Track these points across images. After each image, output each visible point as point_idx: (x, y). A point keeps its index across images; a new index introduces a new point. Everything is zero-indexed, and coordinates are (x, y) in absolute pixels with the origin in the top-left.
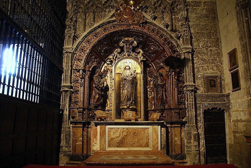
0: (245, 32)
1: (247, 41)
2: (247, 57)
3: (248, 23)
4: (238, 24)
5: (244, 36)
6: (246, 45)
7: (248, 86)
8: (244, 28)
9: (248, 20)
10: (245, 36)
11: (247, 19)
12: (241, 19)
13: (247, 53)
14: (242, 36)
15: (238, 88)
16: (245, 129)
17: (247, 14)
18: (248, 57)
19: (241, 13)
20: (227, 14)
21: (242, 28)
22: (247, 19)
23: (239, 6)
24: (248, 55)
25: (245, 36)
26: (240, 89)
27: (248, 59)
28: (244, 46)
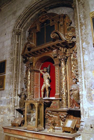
0: (15, 50)
1: (15, 57)
2: (13, 68)
3: (18, 45)
4: (12, 44)
5: (13, 53)
6: (14, 60)
7: (10, 89)
8: (15, 47)
9: (18, 43)
10: (14, 53)
11: (18, 42)
12: (15, 41)
13: (14, 65)
14: (12, 53)
15: (2, 89)
16: (3, 121)
17: (19, 39)
18: (13, 68)
19: (15, 37)
20: (5, 34)
21: (14, 47)
22: (18, 42)
23: (14, 32)
24: (14, 67)
25: (14, 53)
26: (4, 90)
27: (13, 69)
28: (12, 60)
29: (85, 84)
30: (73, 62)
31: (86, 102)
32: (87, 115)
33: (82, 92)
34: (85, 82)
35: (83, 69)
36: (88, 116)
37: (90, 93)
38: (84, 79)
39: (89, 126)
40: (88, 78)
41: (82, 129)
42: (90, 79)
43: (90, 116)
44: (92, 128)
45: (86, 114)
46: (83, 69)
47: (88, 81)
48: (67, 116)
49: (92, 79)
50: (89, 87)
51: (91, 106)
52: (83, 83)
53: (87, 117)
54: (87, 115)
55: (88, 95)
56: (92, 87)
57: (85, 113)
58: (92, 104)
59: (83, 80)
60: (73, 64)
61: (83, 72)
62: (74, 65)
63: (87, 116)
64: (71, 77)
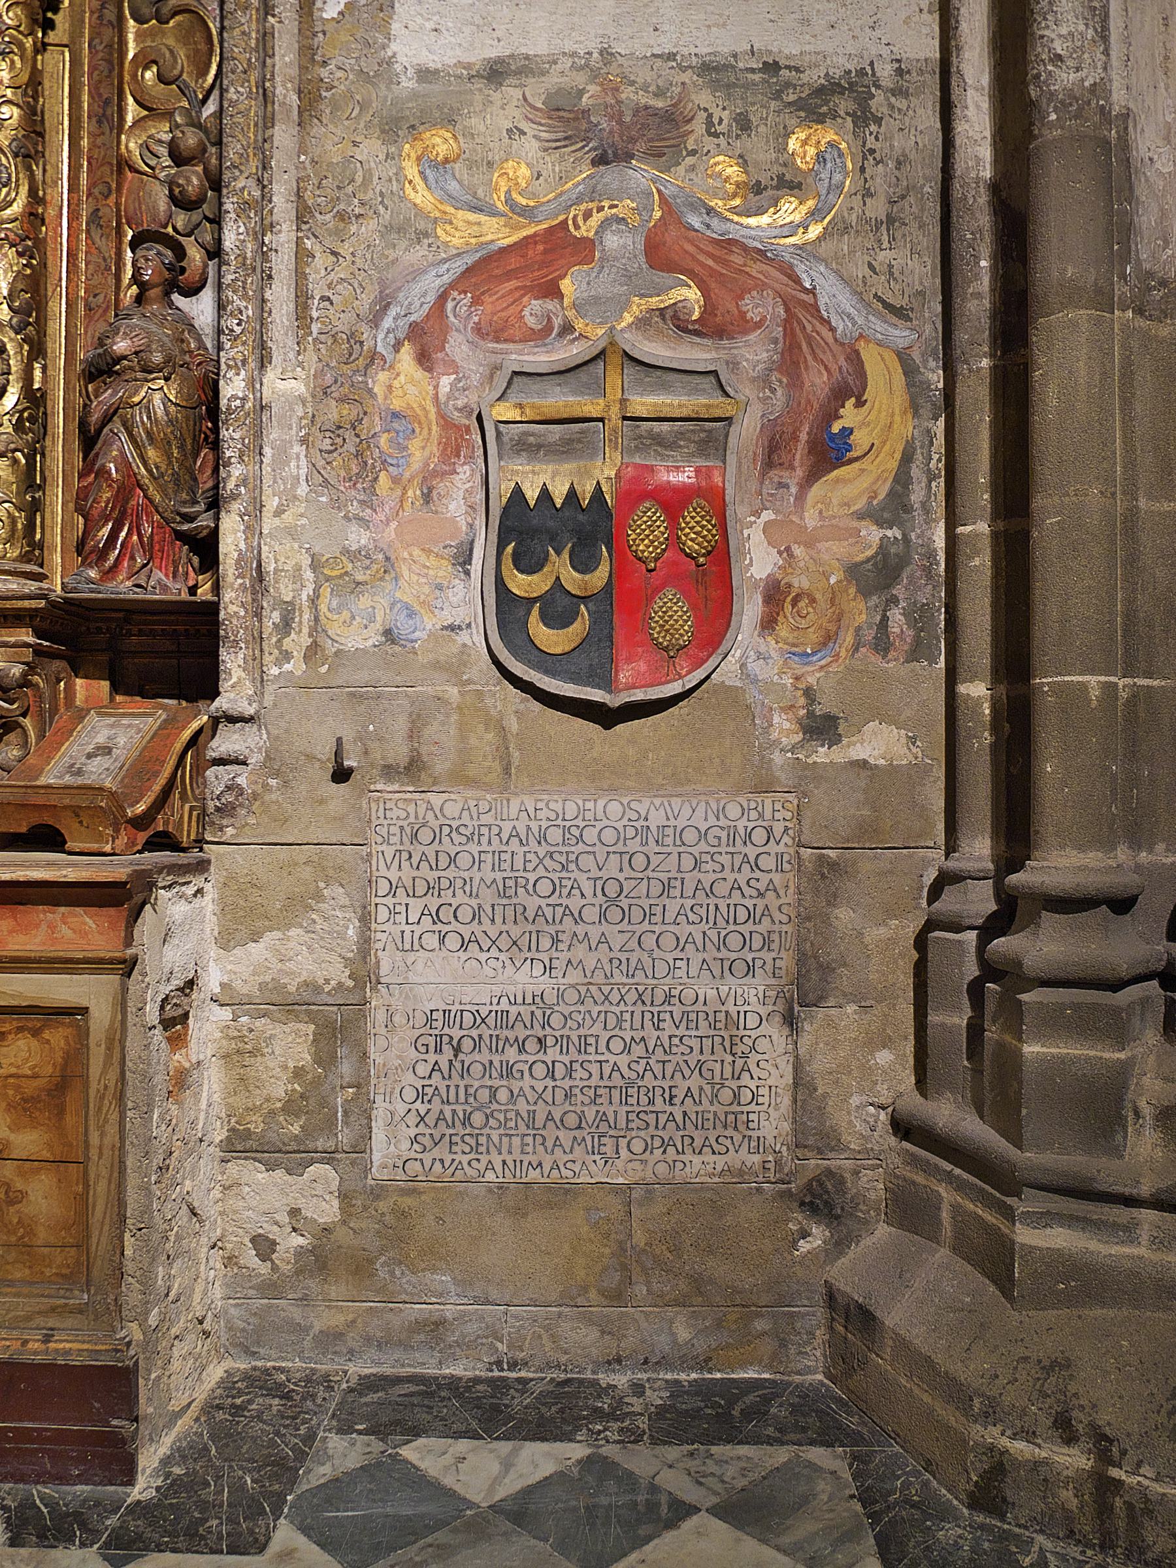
29: (300, 277)
30: (139, 36)
31: (302, 490)
32: (298, 641)
33: (251, 383)
34: (302, 255)
35: (285, 93)
36: (313, 652)
37: (357, 396)
38: (300, 220)
39: (310, 757)
40: (342, 217)
41: (229, 798)
42: (368, 229)
43: (331, 648)
44: (341, 775)
45: (285, 626)
46: (285, 93)
47: (345, 249)
48: (31, 668)
49: (389, 228)
50: (343, 322)
51: (358, 538)
52: (282, 263)
53: (295, 666)
54: (298, 641)
55: (333, 412)
56: (388, 322)
57: (276, 616)
58: (364, 523)
59: (283, 238)
60: (145, 60)
61: (283, 136)
62: (160, 78)
63: (298, 655)
64: (108, 212)
